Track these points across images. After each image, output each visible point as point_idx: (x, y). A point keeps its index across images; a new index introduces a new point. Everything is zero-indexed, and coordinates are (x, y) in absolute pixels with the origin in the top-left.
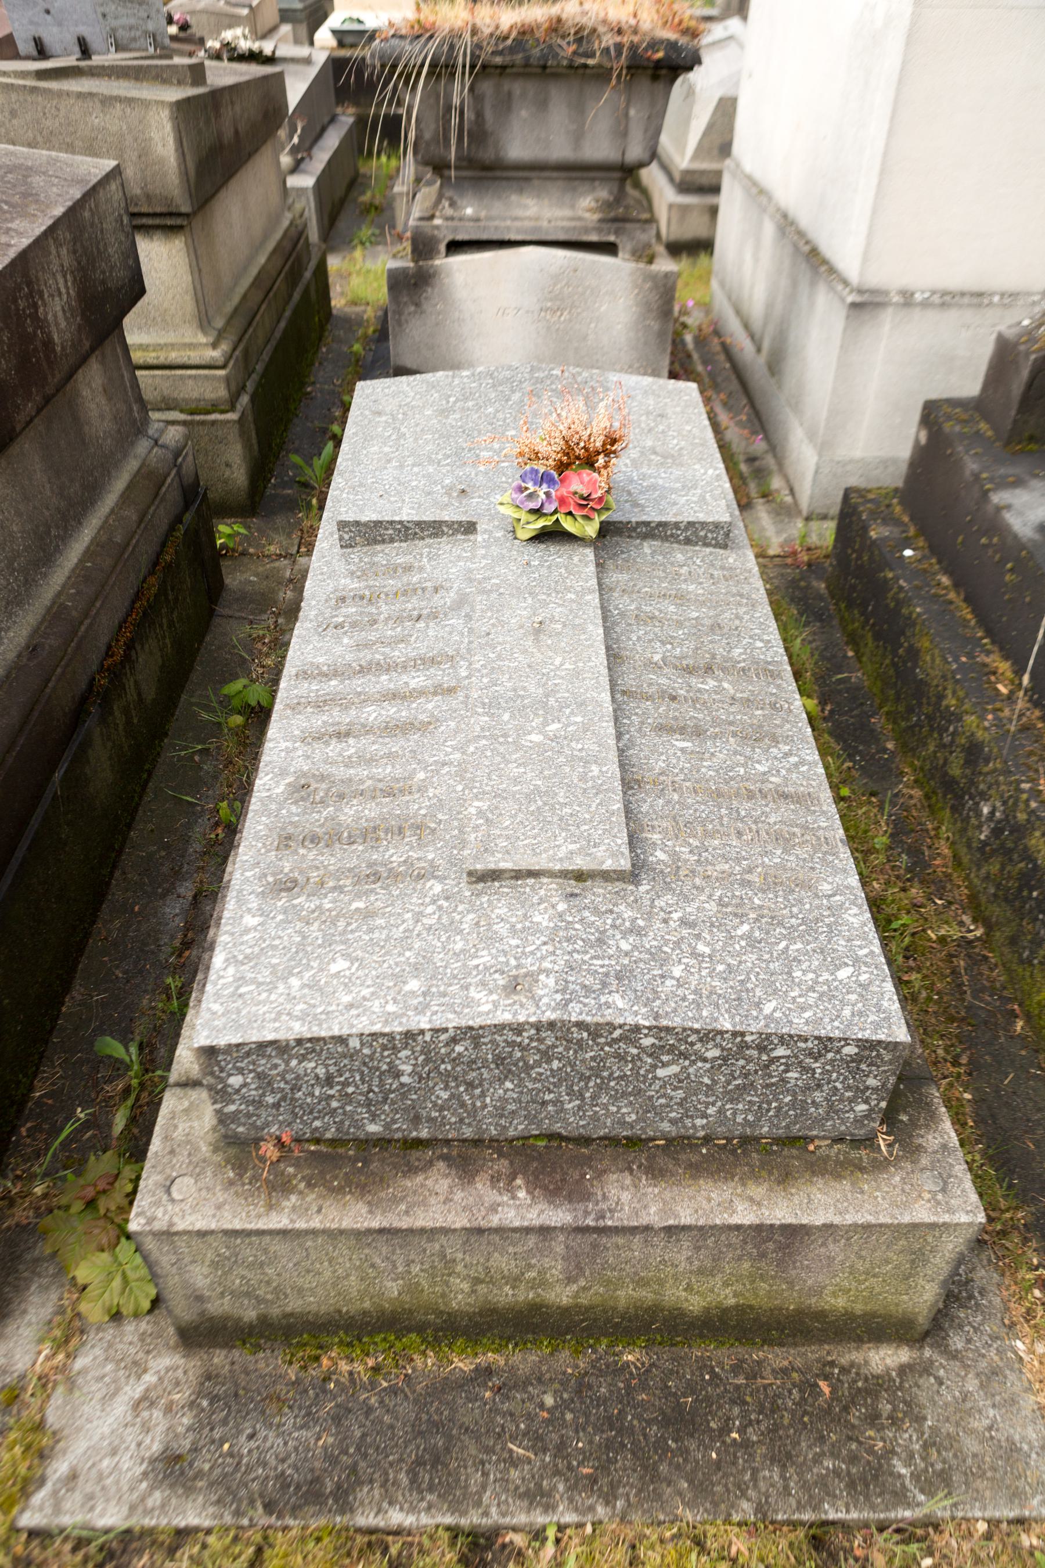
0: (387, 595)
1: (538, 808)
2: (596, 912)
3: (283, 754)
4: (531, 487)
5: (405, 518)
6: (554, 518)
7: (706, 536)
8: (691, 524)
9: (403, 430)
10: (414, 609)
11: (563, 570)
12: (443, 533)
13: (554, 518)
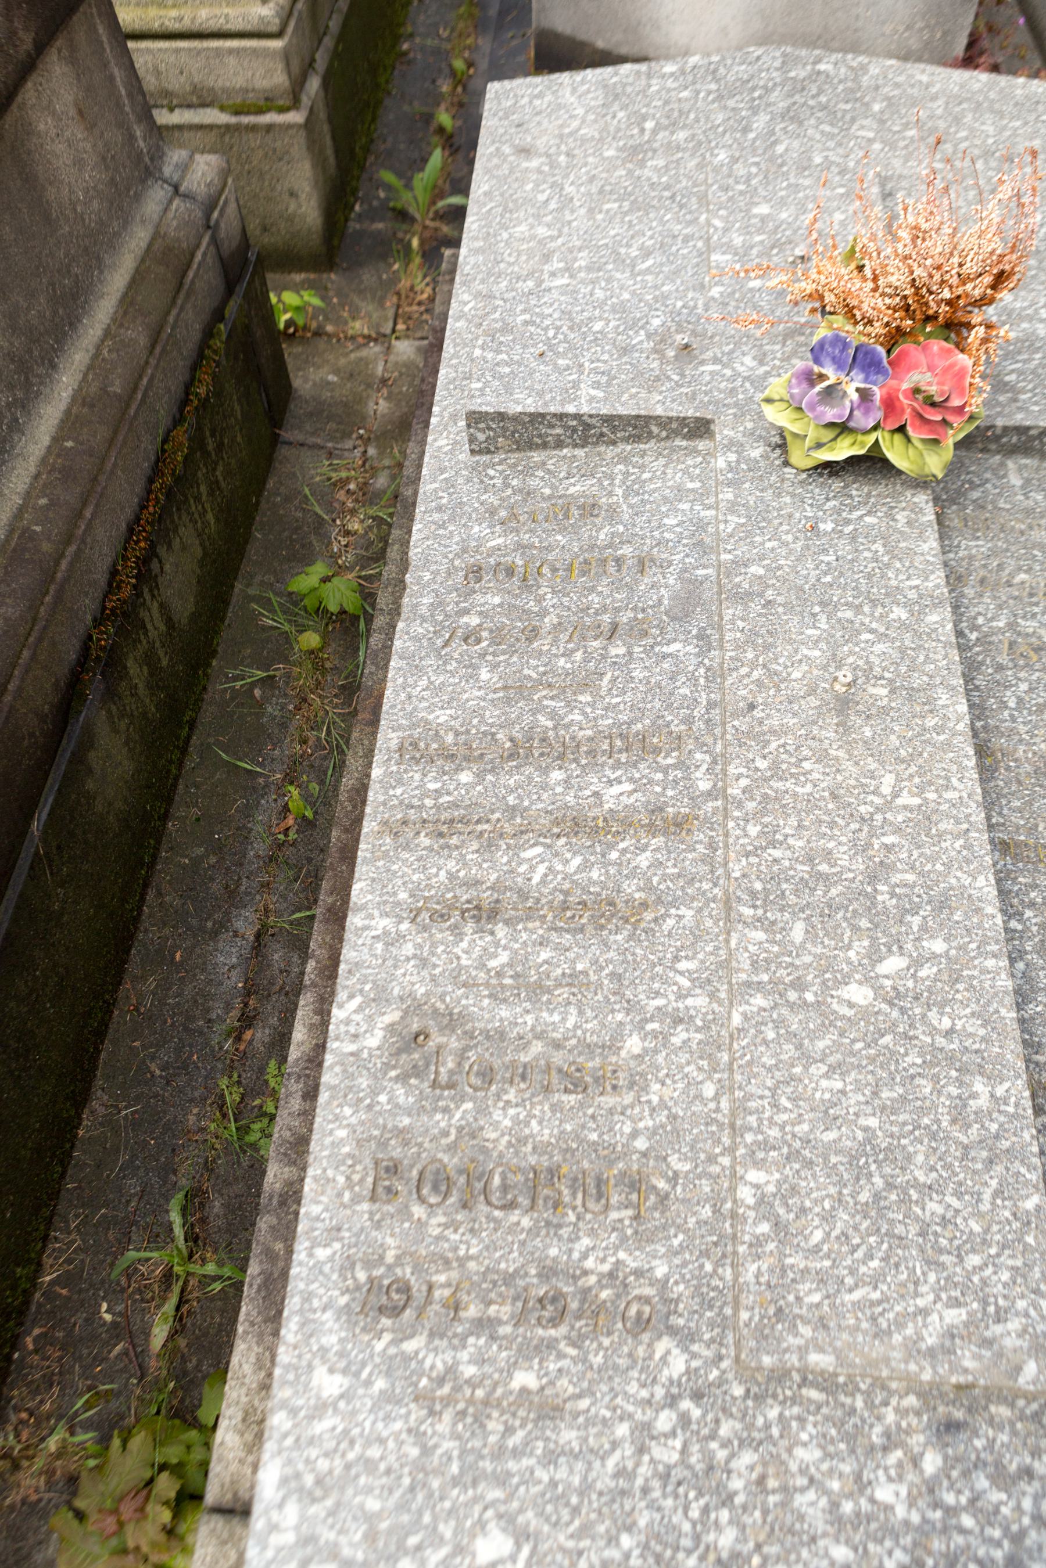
0: (554, 570)
1: (877, 1197)
2: (1001, 1478)
3: (379, 946)
4: (832, 375)
5: (585, 409)
6: (871, 439)
9: (569, 189)
10: (604, 609)
11: (878, 546)
12: (650, 435)
13: (871, 439)
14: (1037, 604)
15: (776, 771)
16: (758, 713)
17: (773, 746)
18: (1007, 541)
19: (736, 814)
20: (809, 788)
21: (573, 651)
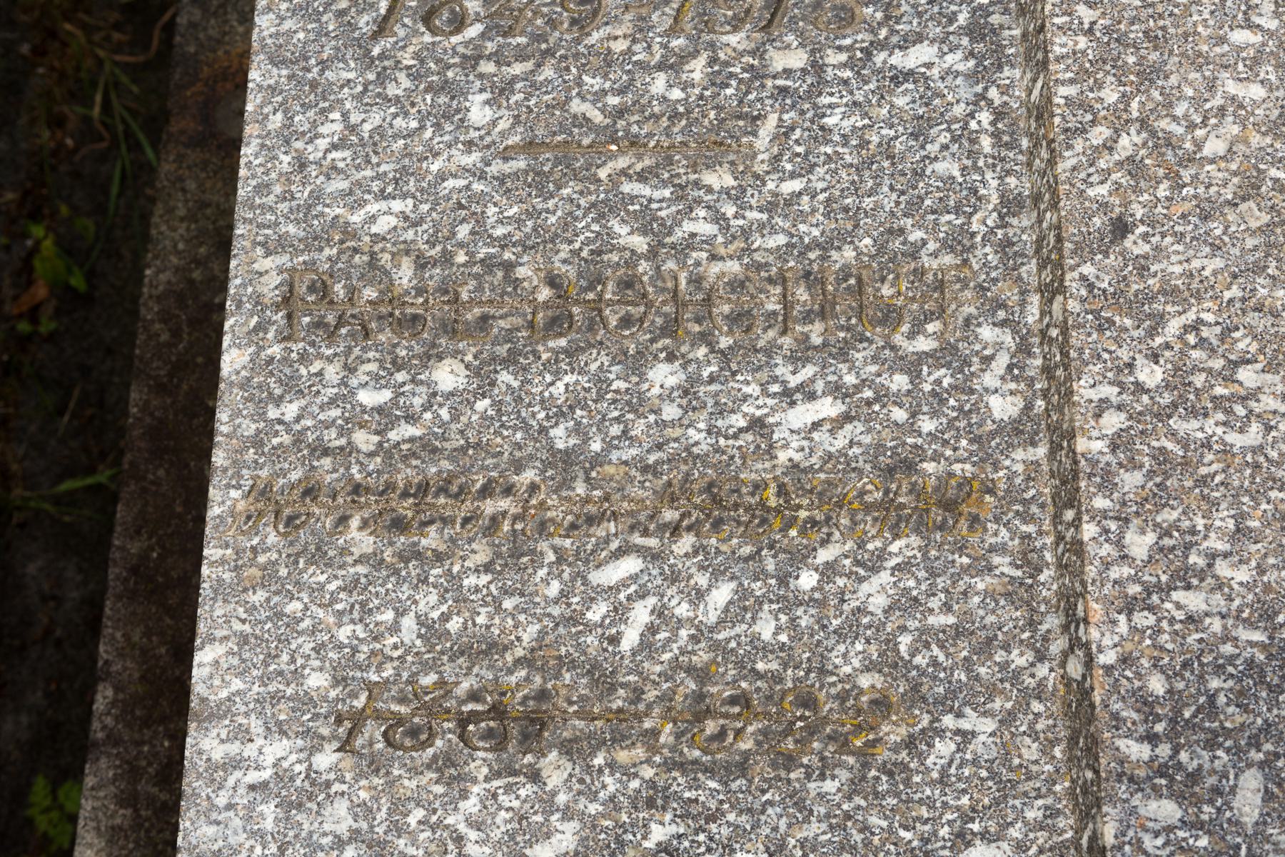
3: (269, 812)
15: (1183, 395)
16: (1135, 245)
17: (1173, 327)
19: (1100, 503)
20: (1254, 434)
21: (686, 57)
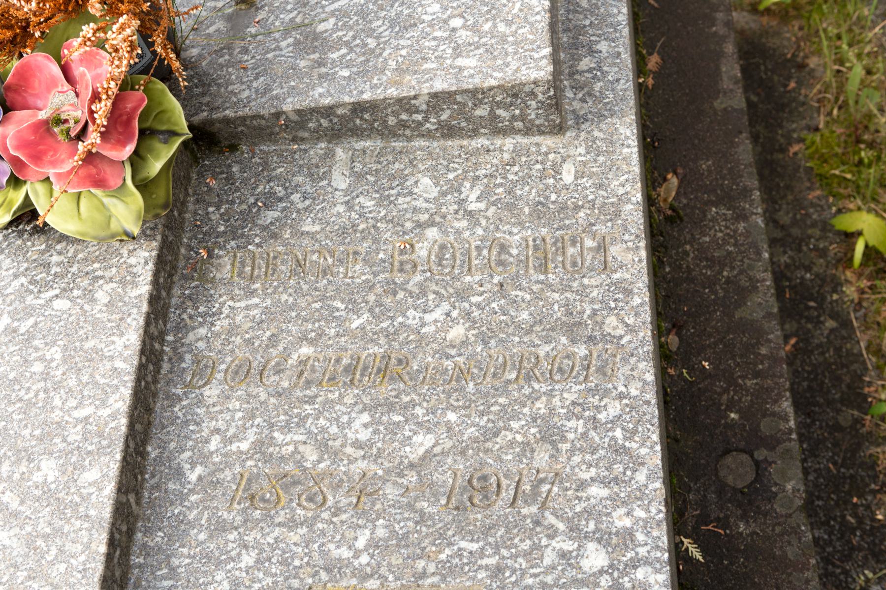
7: (493, 116)
8: (438, 99)
14: (311, 400)
18: (298, 291)
